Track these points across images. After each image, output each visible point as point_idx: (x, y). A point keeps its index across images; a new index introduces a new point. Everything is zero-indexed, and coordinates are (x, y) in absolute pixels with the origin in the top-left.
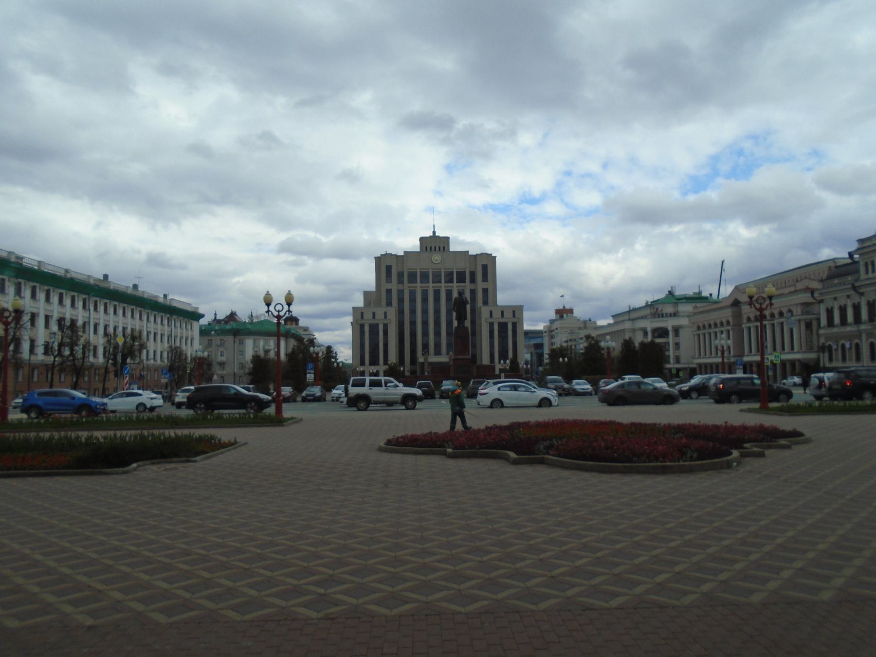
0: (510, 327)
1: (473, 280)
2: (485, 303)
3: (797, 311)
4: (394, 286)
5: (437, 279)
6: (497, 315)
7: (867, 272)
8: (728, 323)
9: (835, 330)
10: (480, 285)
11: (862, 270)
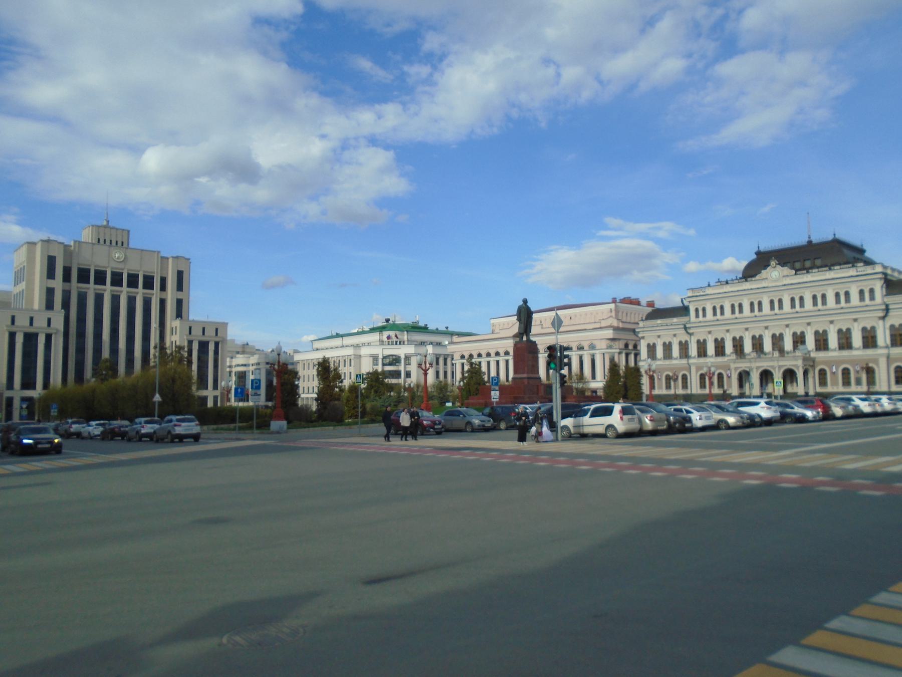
0: (211, 347)
1: (163, 288)
2: (179, 314)
3: (603, 345)
4: (58, 284)
5: (133, 281)
6: (197, 332)
7: (697, 316)
8: (507, 353)
9: (674, 362)
10: (171, 295)
11: (692, 313)
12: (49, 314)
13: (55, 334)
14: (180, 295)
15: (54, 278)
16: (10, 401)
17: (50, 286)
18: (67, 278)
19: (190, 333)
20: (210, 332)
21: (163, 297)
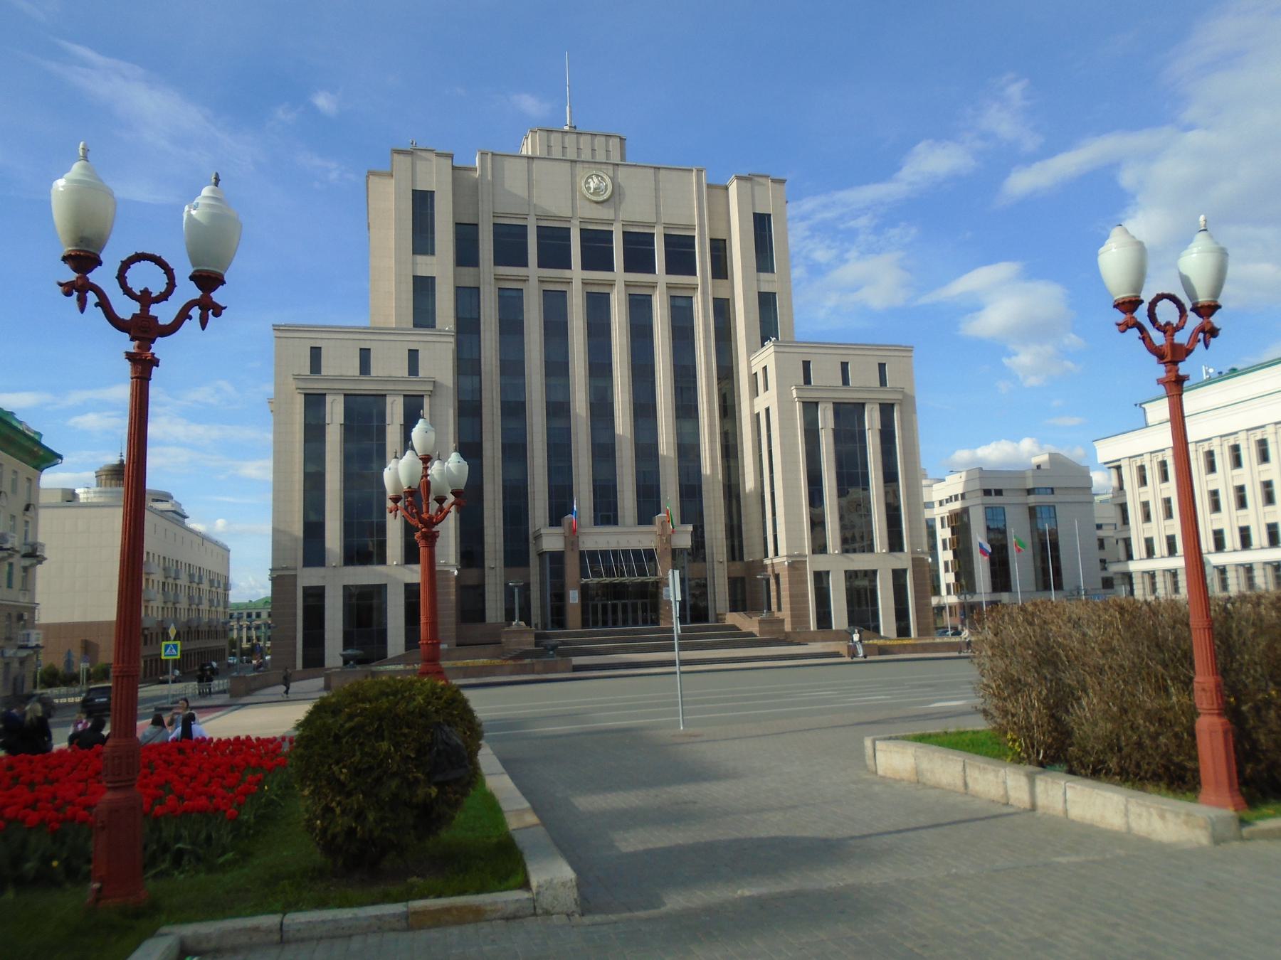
0: (872, 420)
1: (720, 268)
4: (441, 265)
6: (825, 375)
12: (419, 340)
13: (432, 394)
14: (768, 283)
15: (433, 253)
16: (315, 597)
17: (422, 272)
18: (466, 254)
19: (807, 380)
20: (864, 376)
21: (722, 294)
